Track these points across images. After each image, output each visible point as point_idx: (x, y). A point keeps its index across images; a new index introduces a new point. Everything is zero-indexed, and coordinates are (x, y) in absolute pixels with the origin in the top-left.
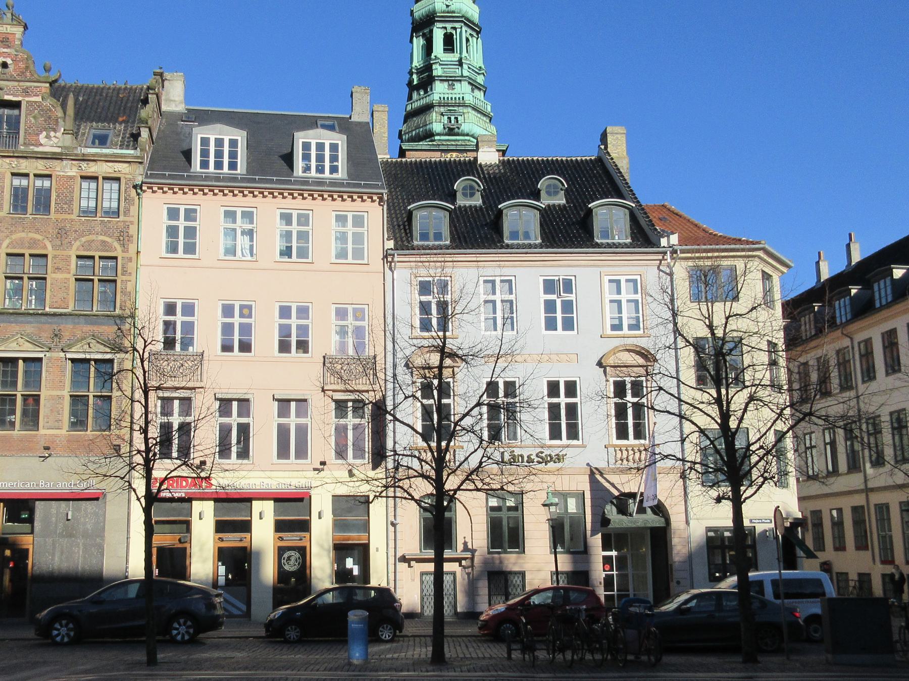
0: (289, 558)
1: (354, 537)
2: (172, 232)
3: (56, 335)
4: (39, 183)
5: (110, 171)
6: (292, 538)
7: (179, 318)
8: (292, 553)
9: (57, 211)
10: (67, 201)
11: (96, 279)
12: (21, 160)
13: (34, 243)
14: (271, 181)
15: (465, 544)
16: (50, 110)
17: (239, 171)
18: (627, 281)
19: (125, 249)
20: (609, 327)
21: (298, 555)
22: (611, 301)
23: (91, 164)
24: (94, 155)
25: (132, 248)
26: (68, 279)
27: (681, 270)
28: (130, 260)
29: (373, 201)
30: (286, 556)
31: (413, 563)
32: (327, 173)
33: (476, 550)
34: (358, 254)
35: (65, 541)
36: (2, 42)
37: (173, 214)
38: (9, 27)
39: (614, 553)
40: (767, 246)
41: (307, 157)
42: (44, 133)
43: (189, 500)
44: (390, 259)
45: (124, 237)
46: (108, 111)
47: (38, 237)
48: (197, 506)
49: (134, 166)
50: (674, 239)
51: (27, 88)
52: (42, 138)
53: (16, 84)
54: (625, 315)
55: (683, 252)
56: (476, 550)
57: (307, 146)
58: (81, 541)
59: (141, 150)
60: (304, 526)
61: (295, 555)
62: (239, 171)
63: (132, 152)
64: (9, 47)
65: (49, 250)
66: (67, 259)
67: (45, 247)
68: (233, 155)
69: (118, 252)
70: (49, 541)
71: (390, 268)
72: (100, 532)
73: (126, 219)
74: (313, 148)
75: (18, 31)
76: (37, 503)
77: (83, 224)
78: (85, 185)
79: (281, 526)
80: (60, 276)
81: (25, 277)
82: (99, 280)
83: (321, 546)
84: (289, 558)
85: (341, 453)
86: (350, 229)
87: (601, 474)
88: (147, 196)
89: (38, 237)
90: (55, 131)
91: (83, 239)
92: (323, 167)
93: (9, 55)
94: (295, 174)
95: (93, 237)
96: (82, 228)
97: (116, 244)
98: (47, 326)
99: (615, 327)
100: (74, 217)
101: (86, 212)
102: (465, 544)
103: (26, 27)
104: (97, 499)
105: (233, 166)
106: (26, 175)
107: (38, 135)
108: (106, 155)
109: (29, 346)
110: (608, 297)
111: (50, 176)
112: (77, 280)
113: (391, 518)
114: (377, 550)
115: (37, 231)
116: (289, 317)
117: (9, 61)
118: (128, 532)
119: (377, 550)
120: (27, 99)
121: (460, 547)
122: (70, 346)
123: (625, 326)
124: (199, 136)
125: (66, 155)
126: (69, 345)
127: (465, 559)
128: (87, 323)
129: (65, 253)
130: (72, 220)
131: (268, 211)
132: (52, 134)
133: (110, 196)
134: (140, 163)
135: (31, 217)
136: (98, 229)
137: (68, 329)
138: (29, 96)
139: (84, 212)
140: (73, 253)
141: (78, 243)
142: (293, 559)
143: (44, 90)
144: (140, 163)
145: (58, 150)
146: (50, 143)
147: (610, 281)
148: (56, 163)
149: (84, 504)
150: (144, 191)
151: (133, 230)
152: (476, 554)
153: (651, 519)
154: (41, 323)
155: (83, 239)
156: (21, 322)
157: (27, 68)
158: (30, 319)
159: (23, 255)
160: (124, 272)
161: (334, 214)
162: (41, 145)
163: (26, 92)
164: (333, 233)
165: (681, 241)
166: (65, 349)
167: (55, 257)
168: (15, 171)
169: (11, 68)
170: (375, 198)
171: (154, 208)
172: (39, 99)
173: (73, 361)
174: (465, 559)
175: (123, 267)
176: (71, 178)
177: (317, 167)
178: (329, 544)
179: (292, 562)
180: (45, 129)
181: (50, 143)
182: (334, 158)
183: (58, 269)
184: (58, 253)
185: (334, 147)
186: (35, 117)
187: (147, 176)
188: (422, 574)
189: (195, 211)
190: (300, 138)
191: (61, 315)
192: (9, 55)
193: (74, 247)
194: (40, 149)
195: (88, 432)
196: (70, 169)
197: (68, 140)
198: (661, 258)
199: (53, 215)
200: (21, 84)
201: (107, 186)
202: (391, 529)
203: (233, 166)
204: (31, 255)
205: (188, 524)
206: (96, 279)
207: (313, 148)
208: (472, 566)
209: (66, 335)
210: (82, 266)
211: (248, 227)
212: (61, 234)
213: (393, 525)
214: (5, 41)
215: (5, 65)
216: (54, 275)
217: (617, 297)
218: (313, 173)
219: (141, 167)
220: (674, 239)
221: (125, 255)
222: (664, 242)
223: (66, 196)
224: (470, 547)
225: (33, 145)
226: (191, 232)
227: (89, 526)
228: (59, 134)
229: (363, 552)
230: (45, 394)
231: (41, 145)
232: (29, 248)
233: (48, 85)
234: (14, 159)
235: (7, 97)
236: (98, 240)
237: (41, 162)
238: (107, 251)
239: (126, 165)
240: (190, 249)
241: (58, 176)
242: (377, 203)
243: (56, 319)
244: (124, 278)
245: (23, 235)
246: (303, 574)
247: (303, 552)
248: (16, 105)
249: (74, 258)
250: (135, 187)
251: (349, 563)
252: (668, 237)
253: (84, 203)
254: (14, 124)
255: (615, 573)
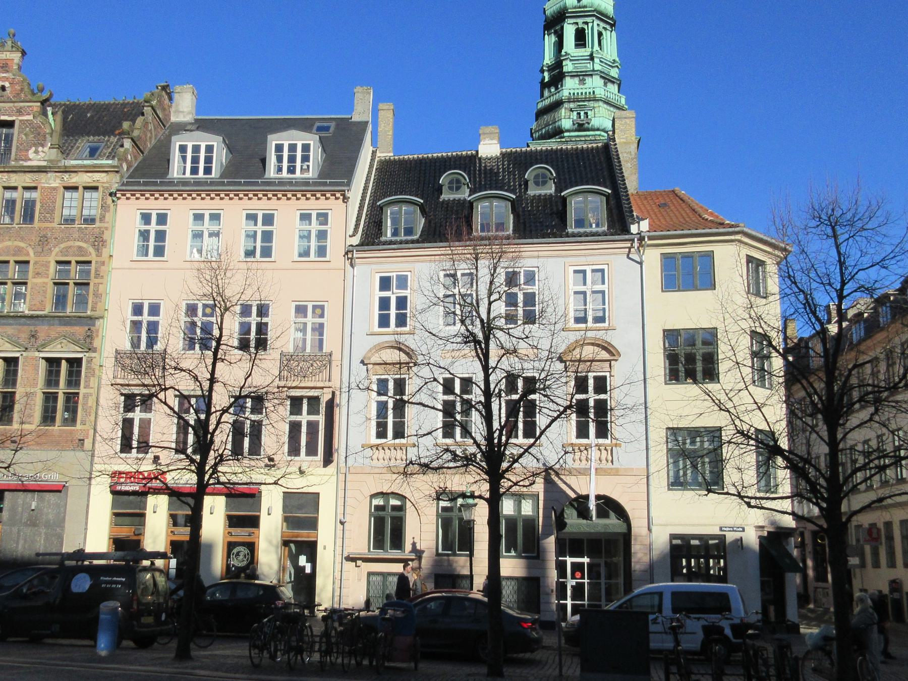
0: (238, 554)
1: (304, 535)
2: (144, 235)
3: (33, 336)
4: (27, 195)
5: (90, 180)
6: (241, 534)
7: (146, 318)
8: (241, 548)
9: (40, 220)
10: (49, 210)
11: (71, 282)
12: (12, 175)
13: (19, 250)
14: (239, 184)
15: (414, 544)
16: (40, 127)
17: (213, 175)
18: (593, 271)
19: (99, 254)
20: (572, 320)
21: (247, 551)
22: (576, 293)
23: (73, 174)
24: (74, 167)
25: (105, 252)
26: (46, 283)
27: (653, 257)
28: (103, 263)
29: (337, 199)
30: (235, 551)
31: (359, 563)
32: (298, 174)
33: (423, 552)
34: (322, 251)
35: (28, 531)
36: (2, 67)
37: (146, 218)
38: (8, 53)
39: (586, 560)
40: (745, 229)
41: (280, 159)
42: (34, 149)
43: (144, 494)
44: (350, 256)
45: (99, 242)
46: (88, 125)
47: (22, 245)
48: (151, 500)
49: (112, 175)
50: (645, 225)
51: (21, 108)
52: (31, 154)
53: (11, 105)
54: (590, 306)
55: (650, 238)
56: (423, 552)
57: (279, 148)
58: (43, 531)
59: (119, 160)
60: (253, 522)
61: (243, 550)
62: (213, 175)
63: (110, 162)
64: (7, 72)
65: (32, 257)
66: (46, 265)
67: (28, 254)
68: (209, 160)
69: (93, 257)
70: (15, 529)
71: (352, 265)
72: (60, 522)
73: (102, 225)
74: (286, 149)
75: (16, 57)
76: (6, 493)
77: (62, 231)
78: (68, 194)
79: (234, 521)
80: (39, 280)
81: (9, 282)
82: (76, 284)
83: (270, 542)
84: (238, 554)
85: (294, 450)
86: (315, 227)
87: (557, 474)
88: (122, 202)
89: (22, 245)
90: (43, 146)
91: (62, 246)
92: (294, 167)
93: (7, 79)
94: (266, 176)
95: (71, 243)
96: (62, 235)
97: (91, 250)
98: (26, 327)
99: (578, 320)
100: (55, 225)
101: (70, 221)
102: (414, 544)
103: (24, 53)
104: (60, 491)
105: (208, 170)
106: (15, 188)
107: (27, 151)
108: (85, 166)
109: (8, 346)
110: (572, 288)
111: (35, 188)
112: (55, 284)
113: (340, 517)
114: (325, 548)
115: (22, 239)
116: (250, 315)
117: (7, 84)
118: (86, 524)
119: (325, 548)
120: (20, 118)
121: (408, 547)
122: (44, 346)
123: (590, 319)
124: (178, 144)
125: (50, 167)
126: (42, 345)
127: (412, 560)
128: (61, 324)
129: (44, 259)
130: (53, 228)
131: (235, 212)
132: (40, 149)
133: (92, 203)
134: (117, 172)
135: (17, 226)
136: (76, 235)
137: (43, 330)
138: (23, 115)
139: (66, 220)
140: (52, 260)
141: (57, 249)
142: (242, 554)
143: (35, 109)
144: (117, 172)
145: (44, 164)
146: (37, 157)
147: (575, 272)
148: (43, 175)
149: (47, 495)
150: (119, 198)
151: (106, 236)
152: (424, 555)
153: (613, 523)
154: (20, 324)
155: (62, 246)
156: (4, 324)
157: (22, 90)
158: (11, 321)
159: (7, 262)
160: (97, 275)
161: (298, 213)
162: (30, 160)
163: (20, 112)
164: (297, 231)
165: (652, 228)
166: (40, 349)
167: (36, 263)
168: (6, 185)
169: (8, 91)
170: (338, 195)
171: (127, 216)
172: (30, 117)
173: (47, 360)
174: (412, 560)
175: (96, 270)
176: (54, 189)
177: (289, 167)
178: (277, 539)
179: (241, 557)
180: (35, 145)
181: (37, 157)
182: (305, 159)
183: (38, 274)
184: (38, 259)
185: (306, 148)
186: (26, 135)
187: (123, 185)
188: (370, 574)
189: (166, 215)
190: (273, 140)
191: (38, 317)
192: (7, 79)
193: (54, 253)
194: (29, 163)
195: (56, 428)
196: (53, 181)
197: (54, 154)
198: (629, 245)
199: (37, 224)
200: (16, 104)
201: (87, 195)
202: (340, 527)
203: (208, 170)
204: (16, 262)
205: (143, 515)
206: (71, 282)
207: (286, 149)
208: (420, 568)
209: (41, 335)
210: (60, 271)
211: (215, 228)
212: (44, 241)
213: (342, 523)
214: (4, 66)
215: (3, 88)
216: (35, 280)
217: (582, 288)
218: (285, 174)
219: (118, 176)
220: (645, 225)
221: (99, 259)
222: (634, 229)
223: (49, 206)
224: (418, 548)
225: (23, 160)
226: (161, 236)
227: (50, 517)
228: (46, 149)
229: (310, 549)
230: (20, 390)
231: (30, 160)
232: (14, 255)
233: (39, 104)
234: (5, 174)
235: (3, 118)
236: (75, 245)
237: (29, 175)
238: (83, 256)
239: (104, 175)
240: (159, 251)
241: (43, 188)
242: (341, 200)
243: (33, 321)
244: (97, 281)
245: (9, 243)
246: (250, 569)
247: (251, 547)
248: (10, 124)
249: (53, 265)
250: (111, 194)
251: (302, 560)
252: (639, 223)
253: (66, 212)
254: (9, 139)
255: (586, 581)
